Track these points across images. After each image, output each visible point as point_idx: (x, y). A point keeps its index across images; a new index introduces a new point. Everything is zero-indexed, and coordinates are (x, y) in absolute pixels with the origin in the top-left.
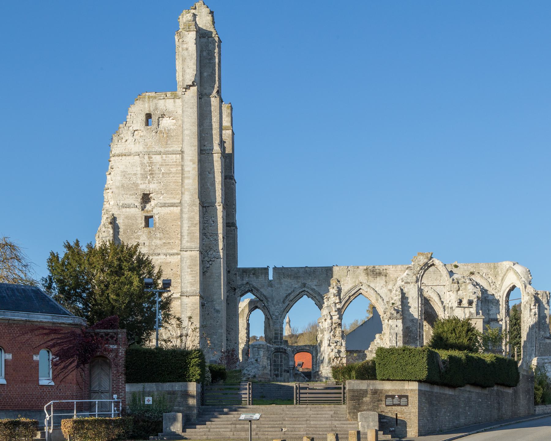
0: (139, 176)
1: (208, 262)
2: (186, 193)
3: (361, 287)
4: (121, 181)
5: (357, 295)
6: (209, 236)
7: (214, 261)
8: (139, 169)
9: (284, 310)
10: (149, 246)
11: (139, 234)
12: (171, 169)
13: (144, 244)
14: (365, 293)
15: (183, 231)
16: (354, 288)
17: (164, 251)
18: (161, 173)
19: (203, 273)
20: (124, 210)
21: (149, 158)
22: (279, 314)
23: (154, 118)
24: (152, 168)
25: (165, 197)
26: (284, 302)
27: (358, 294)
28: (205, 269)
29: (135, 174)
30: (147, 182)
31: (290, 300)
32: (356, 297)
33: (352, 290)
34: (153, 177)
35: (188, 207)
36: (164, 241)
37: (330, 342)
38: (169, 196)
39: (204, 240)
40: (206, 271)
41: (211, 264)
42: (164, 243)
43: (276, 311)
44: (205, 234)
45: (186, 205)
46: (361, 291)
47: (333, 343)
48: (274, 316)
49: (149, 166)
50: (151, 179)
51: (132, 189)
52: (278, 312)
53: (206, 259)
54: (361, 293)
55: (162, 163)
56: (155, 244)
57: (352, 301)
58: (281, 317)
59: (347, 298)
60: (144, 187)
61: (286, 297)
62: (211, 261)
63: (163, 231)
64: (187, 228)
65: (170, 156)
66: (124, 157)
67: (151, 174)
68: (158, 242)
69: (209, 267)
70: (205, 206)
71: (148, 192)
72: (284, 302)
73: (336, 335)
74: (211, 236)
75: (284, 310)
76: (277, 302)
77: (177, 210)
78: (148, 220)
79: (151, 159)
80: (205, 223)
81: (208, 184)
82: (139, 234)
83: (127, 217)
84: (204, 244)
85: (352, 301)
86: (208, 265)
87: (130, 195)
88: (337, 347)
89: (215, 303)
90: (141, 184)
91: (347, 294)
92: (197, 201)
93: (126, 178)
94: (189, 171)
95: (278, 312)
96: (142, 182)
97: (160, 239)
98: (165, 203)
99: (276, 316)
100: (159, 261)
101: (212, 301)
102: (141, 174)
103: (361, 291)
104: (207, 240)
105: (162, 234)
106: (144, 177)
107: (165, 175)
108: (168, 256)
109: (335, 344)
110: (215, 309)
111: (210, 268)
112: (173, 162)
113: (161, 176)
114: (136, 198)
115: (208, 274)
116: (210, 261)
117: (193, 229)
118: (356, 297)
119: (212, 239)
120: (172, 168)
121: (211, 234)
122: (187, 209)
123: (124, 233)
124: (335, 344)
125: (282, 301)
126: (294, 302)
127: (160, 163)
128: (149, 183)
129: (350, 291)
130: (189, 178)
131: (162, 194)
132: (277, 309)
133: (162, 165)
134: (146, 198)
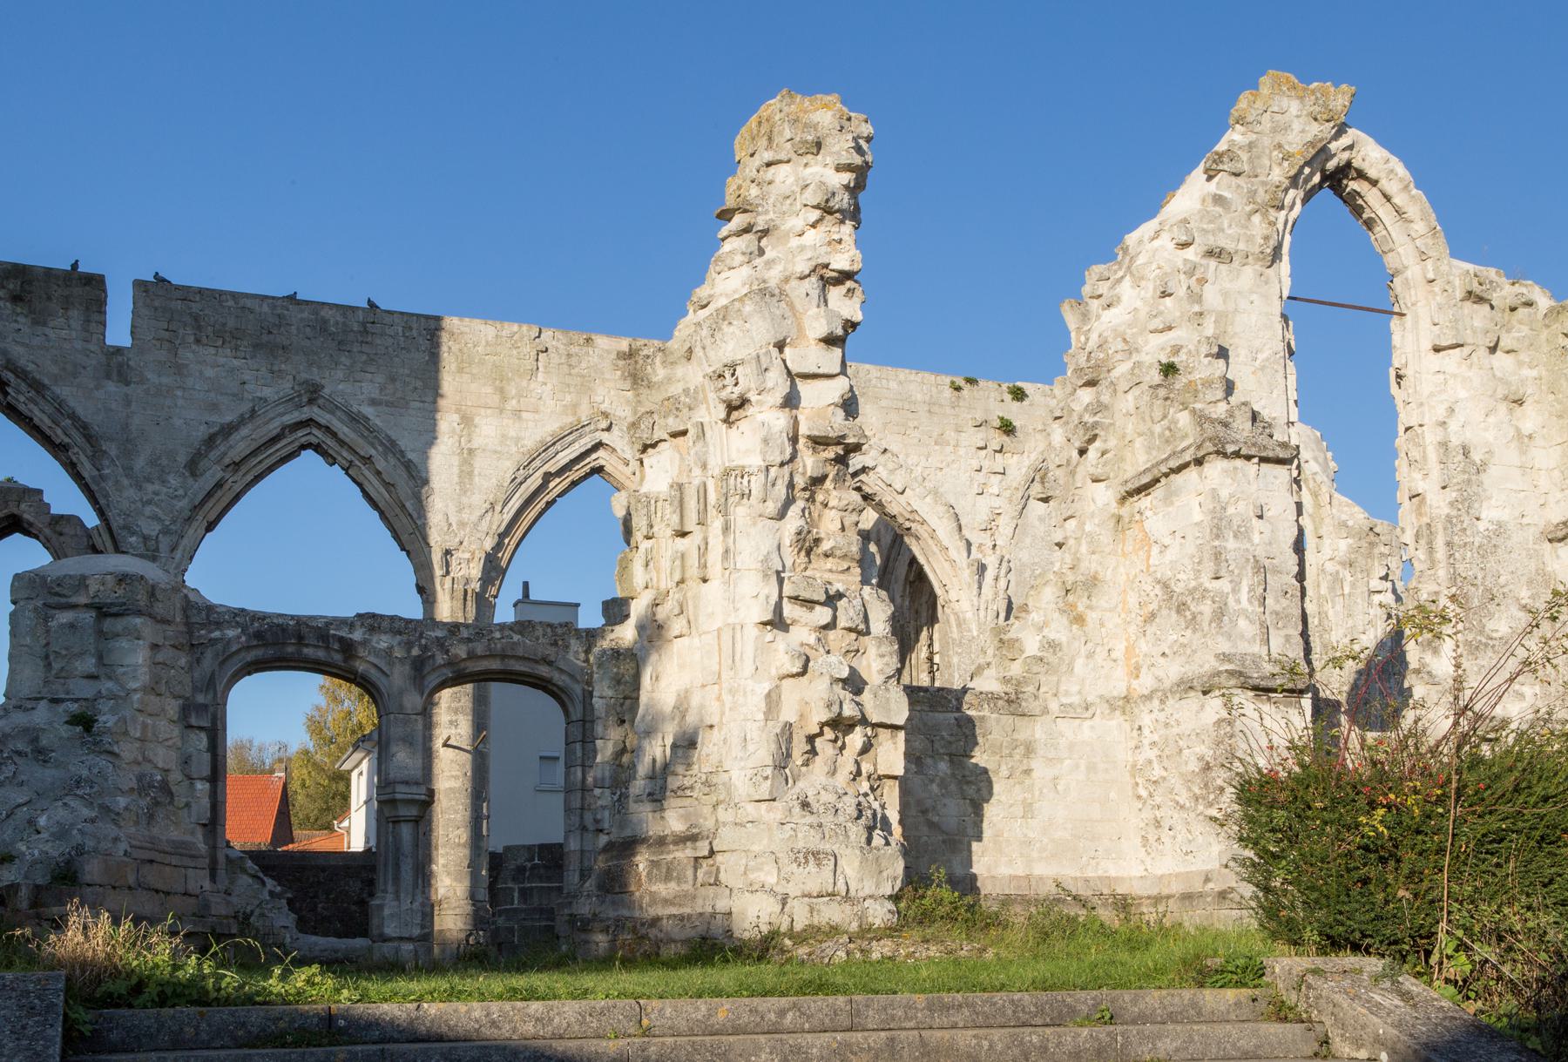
3: (605, 437)
5: (582, 473)
9: (196, 508)
14: (621, 467)
16: (570, 438)
22: (166, 531)
26: (193, 467)
27: (587, 469)
31: (227, 461)
32: (574, 484)
33: (558, 446)
37: (788, 589)
43: (148, 510)
46: (601, 457)
47: (809, 603)
48: (133, 539)
52: (159, 519)
54: (599, 470)
57: (554, 501)
58: (173, 550)
59: (535, 481)
61: (211, 441)
72: (193, 467)
73: (817, 541)
75: (196, 508)
76: (153, 462)
85: (554, 501)
88: (832, 635)
91: (537, 463)
95: (159, 519)
99: (146, 538)
103: (601, 457)
109: (823, 615)
118: (574, 484)
124: (823, 615)
125: (182, 459)
126: (249, 477)
129: (552, 450)
132: (149, 502)
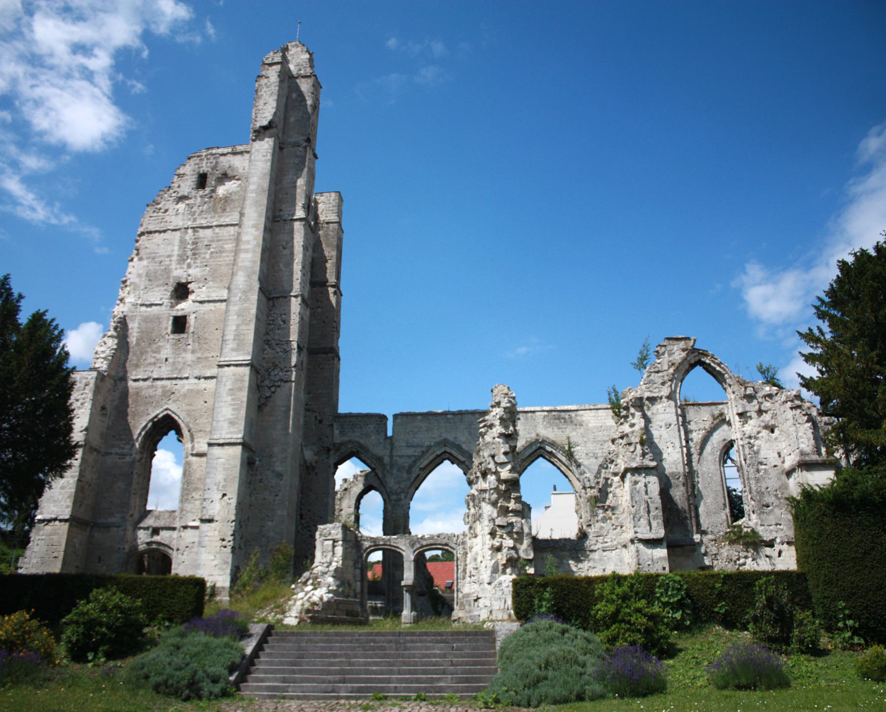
0: (175, 258)
1: (269, 388)
2: (240, 273)
4: (147, 266)
6: (274, 345)
7: (279, 386)
8: (176, 248)
10: (174, 363)
11: (160, 344)
12: (226, 246)
13: (166, 360)
15: (226, 333)
17: (197, 373)
18: (209, 252)
20: (143, 308)
23: (211, 181)
25: (210, 288)
28: (263, 401)
29: (169, 256)
30: (185, 266)
34: (196, 259)
35: (239, 295)
36: (199, 355)
38: (216, 285)
39: (266, 352)
40: (264, 404)
41: (274, 392)
42: (199, 358)
44: (268, 341)
45: (237, 291)
50: (192, 262)
51: (161, 277)
53: (267, 382)
55: (213, 237)
56: (184, 361)
60: (179, 273)
63: (198, 339)
68: (189, 357)
69: (270, 397)
70: (273, 298)
74: (277, 345)
78: (180, 324)
79: (197, 234)
80: (270, 324)
81: (281, 265)
82: (160, 344)
83: (146, 319)
84: (264, 358)
86: (268, 395)
87: (157, 286)
89: (275, 459)
92: (256, 286)
93: (155, 262)
96: (178, 266)
100: (187, 387)
101: (271, 456)
104: (271, 351)
105: (197, 344)
106: (182, 259)
107: (214, 255)
108: (202, 380)
110: (273, 471)
111: (272, 399)
112: (229, 236)
114: (166, 290)
115: (266, 410)
116: (272, 387)
117: (244, 328)
119: (278, 350)
120: (227, 244)
121: (278, 342)
122: (238, 298)
123: (138, 344)
127: (210, 239)
128: (189, 266)
130: (247, 251)
133: (211, 241)
134: (181, 291)
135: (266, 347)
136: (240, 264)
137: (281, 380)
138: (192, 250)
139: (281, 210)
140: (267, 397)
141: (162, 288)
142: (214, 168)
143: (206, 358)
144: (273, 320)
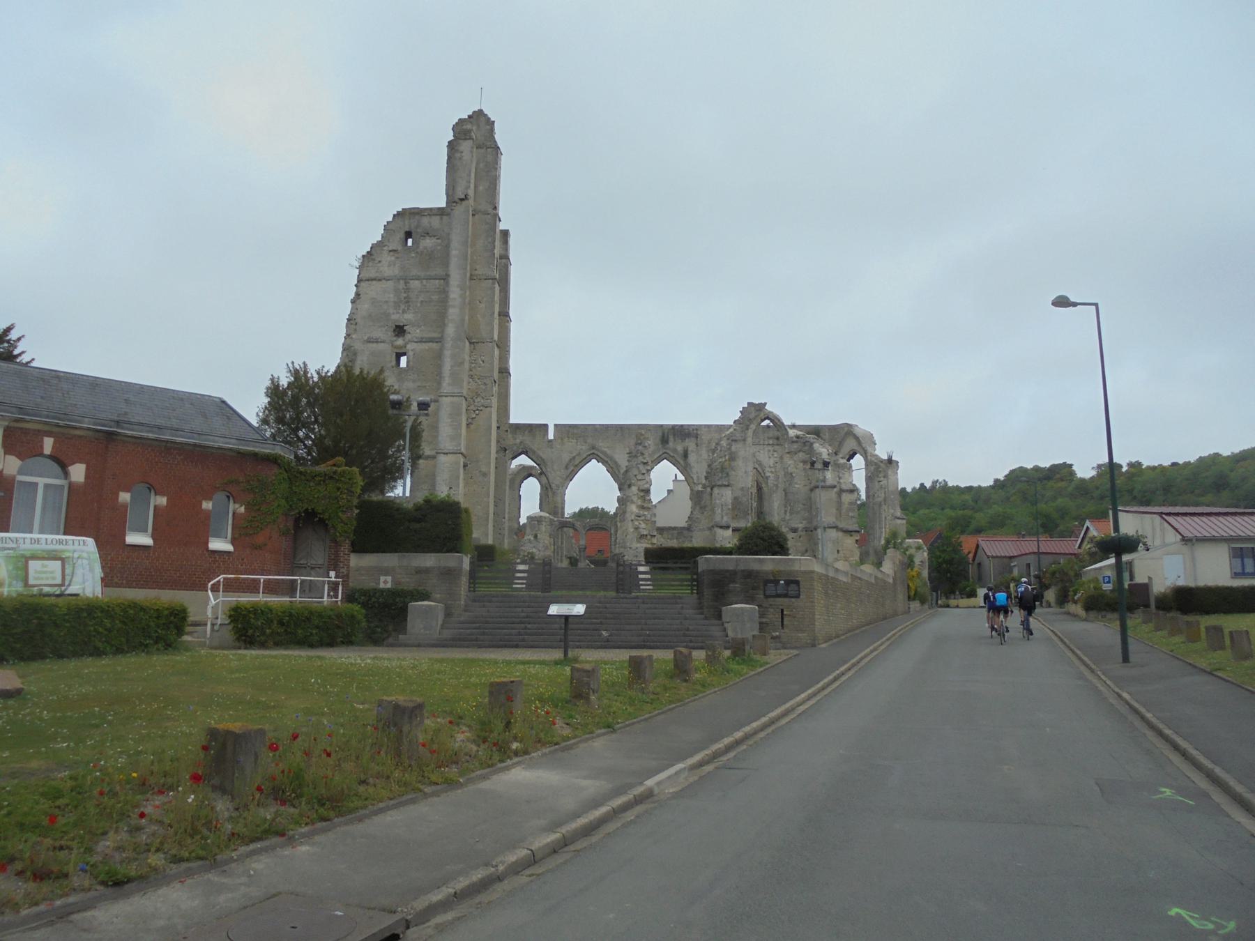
1: (474, 411)
8: (392, 296)
12: (433, 297)
19: (467, 424)
21: (405, 283)
24: (408, 295)
28: (470, 420)
29: (386, 302)
30: (401, 312)
41: (477, 415)
42: (419, 386)
44: (472, 376)
49: (405, 292)
53: (472, 407)
60: (398, 317)
62: (478, 410)
64: (449, 368)
65: (432, 281)
66: (374, 282)
67: (408, 302)
71: (402, 324)
77: (434, 345)
86: (474, 416)
90: (394, 314)
94: (455, 299)
97: (414, 381)
98: (422, 338)
102: (395, 302)
106: (397, 305)
113: (419, 305)
128: (404, 312)
130: (453, 307)
131: (419, 327)
133: (420, 292)
135: (471, 380)
136: (450, 318)
137: (483, 406)
138: (405, 298)
139: (476, 270)
140: (473, 418)
141: (384, 329)
142: (417, 227)
143: (425, 387)
144: (475, 360)
